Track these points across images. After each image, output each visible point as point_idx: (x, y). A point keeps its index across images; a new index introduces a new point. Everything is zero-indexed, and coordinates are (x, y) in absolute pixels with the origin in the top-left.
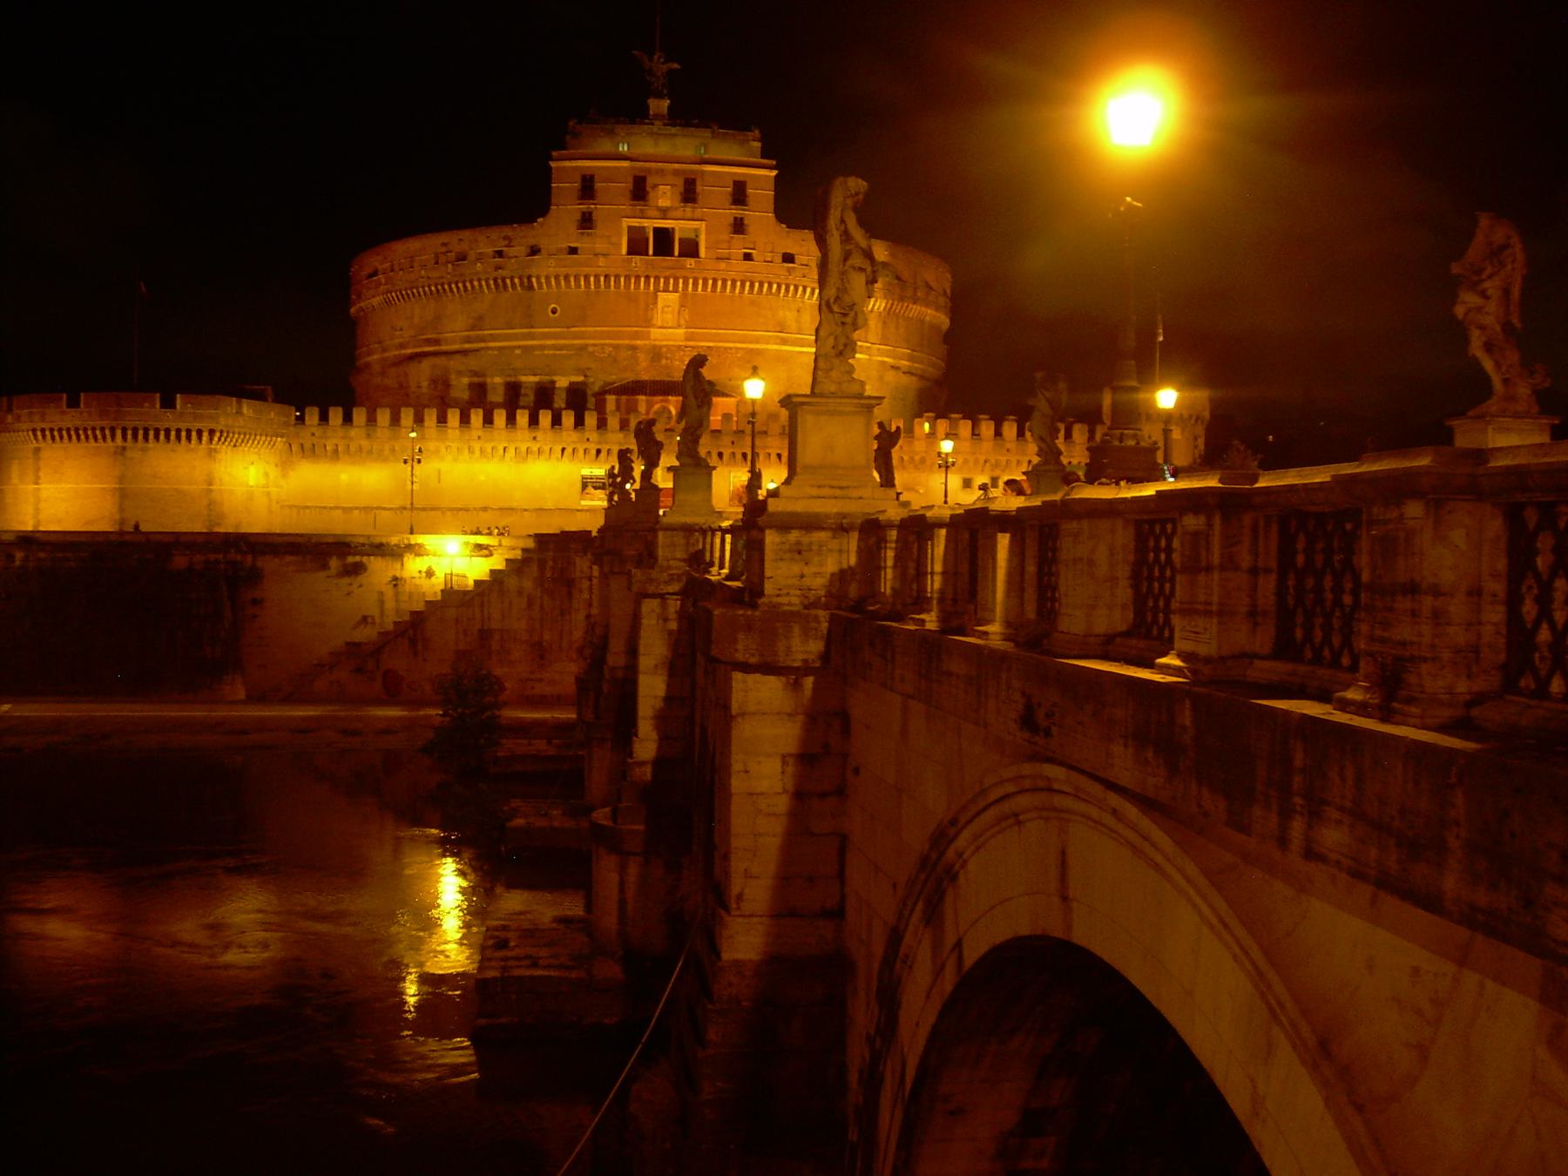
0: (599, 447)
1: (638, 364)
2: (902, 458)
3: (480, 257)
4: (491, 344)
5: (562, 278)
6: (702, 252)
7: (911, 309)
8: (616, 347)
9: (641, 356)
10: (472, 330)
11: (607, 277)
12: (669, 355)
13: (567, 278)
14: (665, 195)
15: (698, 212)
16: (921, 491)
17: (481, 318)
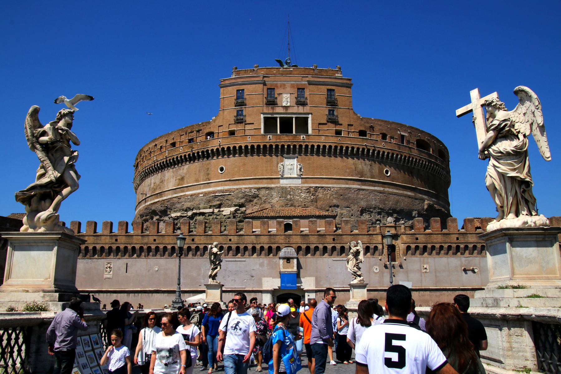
0: (238, 245)
1: (273, 199)
2: (458, 248)
3: (181, 142)
5: (226, 149)
6: (310, 131)
7: (435, 169)
8: (259, 189)
9: (274, 194)
10: (178, 185)
11: (252, 147)
12: (292, 193)
13: (229, 148)
15: (307, 109)
16: (476, 270)
17: (182, 179)
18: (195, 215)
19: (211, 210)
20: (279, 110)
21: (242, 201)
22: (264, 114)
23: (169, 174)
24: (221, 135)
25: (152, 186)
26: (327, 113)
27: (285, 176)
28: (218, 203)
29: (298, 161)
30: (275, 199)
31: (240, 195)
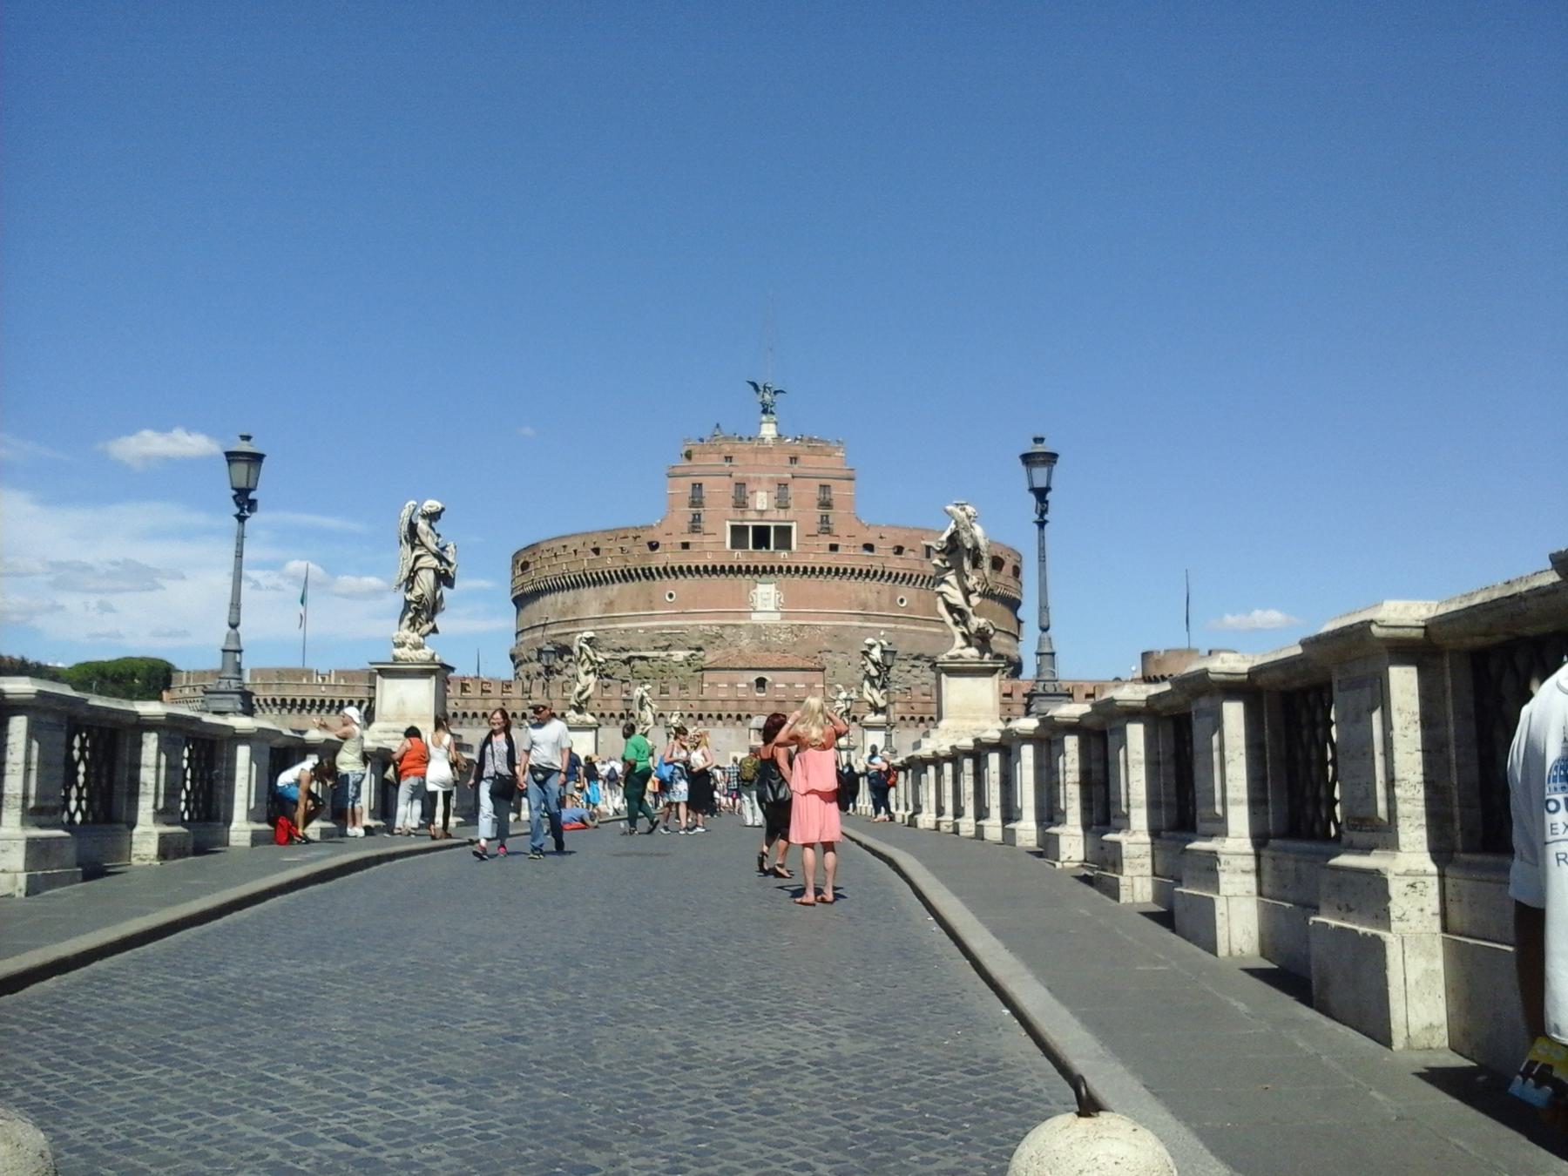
4: (620, 626)
8: (722, 626)
9: (744, 634)
14: (762, 500)
18: (630, 659)
19: (655, 654)
20: (751, 515)
21: (700, 643)
22: (730, 520)
23: (588, 593)
24: (669, 548)
25: (559, 605)
26: (819, 520)
27: (758, 609)
28: (666, 643)
29: (777, 589)
30: (746, 643)
31: (697, 635)
